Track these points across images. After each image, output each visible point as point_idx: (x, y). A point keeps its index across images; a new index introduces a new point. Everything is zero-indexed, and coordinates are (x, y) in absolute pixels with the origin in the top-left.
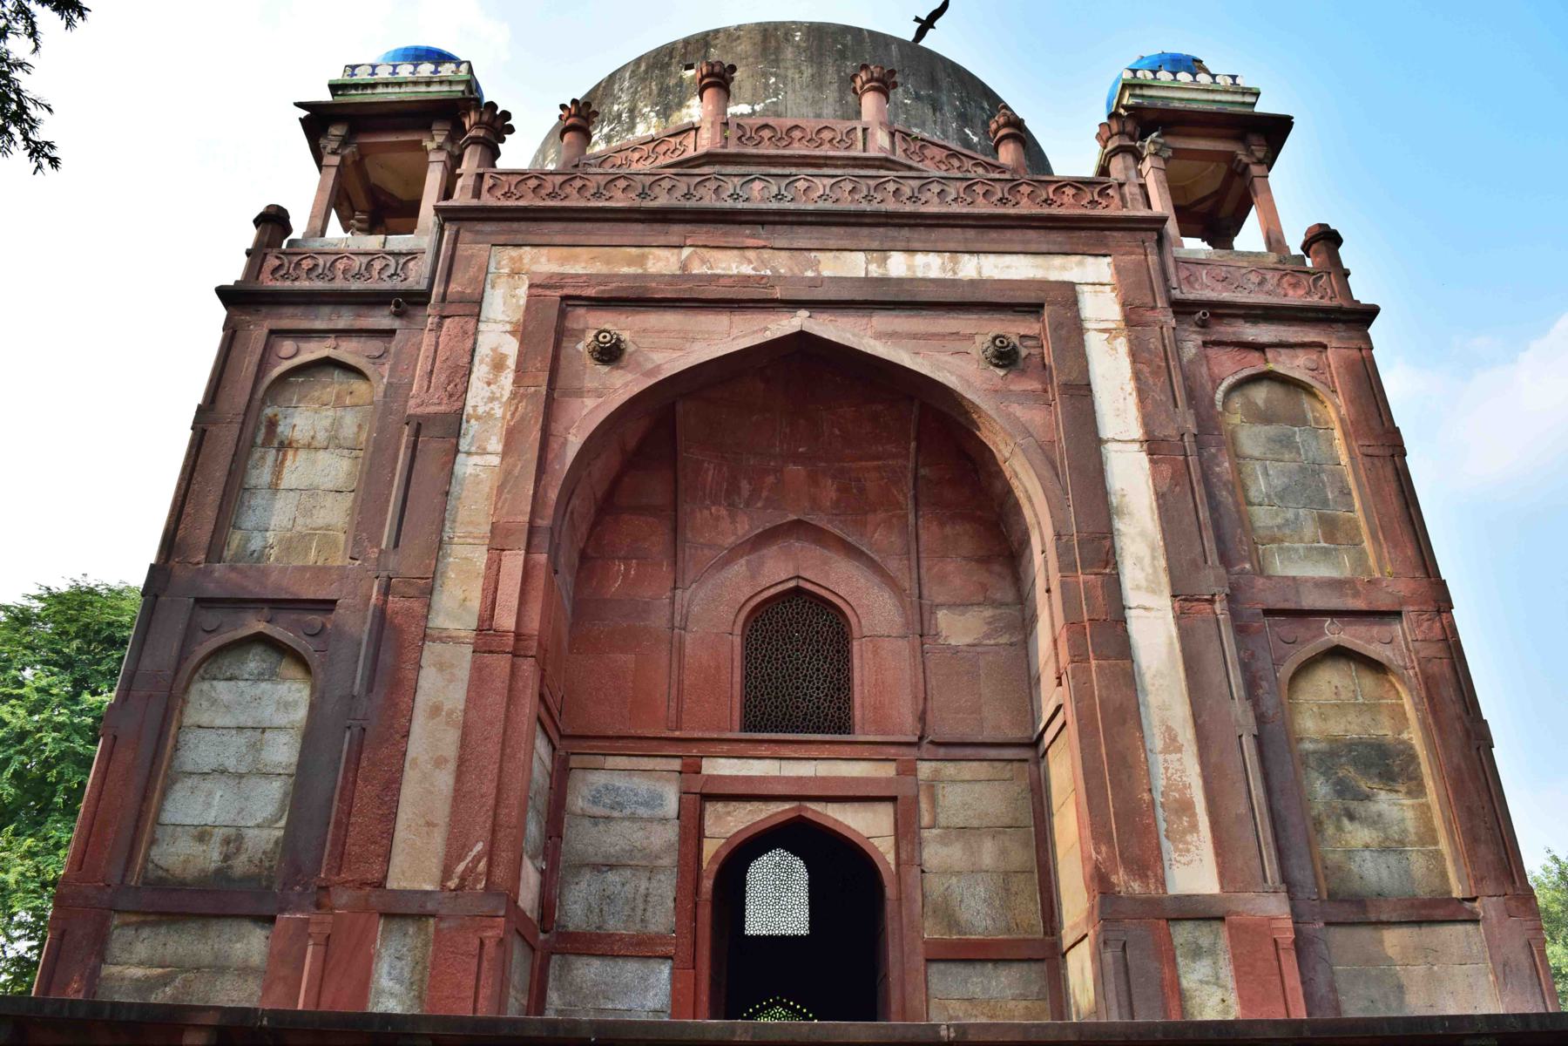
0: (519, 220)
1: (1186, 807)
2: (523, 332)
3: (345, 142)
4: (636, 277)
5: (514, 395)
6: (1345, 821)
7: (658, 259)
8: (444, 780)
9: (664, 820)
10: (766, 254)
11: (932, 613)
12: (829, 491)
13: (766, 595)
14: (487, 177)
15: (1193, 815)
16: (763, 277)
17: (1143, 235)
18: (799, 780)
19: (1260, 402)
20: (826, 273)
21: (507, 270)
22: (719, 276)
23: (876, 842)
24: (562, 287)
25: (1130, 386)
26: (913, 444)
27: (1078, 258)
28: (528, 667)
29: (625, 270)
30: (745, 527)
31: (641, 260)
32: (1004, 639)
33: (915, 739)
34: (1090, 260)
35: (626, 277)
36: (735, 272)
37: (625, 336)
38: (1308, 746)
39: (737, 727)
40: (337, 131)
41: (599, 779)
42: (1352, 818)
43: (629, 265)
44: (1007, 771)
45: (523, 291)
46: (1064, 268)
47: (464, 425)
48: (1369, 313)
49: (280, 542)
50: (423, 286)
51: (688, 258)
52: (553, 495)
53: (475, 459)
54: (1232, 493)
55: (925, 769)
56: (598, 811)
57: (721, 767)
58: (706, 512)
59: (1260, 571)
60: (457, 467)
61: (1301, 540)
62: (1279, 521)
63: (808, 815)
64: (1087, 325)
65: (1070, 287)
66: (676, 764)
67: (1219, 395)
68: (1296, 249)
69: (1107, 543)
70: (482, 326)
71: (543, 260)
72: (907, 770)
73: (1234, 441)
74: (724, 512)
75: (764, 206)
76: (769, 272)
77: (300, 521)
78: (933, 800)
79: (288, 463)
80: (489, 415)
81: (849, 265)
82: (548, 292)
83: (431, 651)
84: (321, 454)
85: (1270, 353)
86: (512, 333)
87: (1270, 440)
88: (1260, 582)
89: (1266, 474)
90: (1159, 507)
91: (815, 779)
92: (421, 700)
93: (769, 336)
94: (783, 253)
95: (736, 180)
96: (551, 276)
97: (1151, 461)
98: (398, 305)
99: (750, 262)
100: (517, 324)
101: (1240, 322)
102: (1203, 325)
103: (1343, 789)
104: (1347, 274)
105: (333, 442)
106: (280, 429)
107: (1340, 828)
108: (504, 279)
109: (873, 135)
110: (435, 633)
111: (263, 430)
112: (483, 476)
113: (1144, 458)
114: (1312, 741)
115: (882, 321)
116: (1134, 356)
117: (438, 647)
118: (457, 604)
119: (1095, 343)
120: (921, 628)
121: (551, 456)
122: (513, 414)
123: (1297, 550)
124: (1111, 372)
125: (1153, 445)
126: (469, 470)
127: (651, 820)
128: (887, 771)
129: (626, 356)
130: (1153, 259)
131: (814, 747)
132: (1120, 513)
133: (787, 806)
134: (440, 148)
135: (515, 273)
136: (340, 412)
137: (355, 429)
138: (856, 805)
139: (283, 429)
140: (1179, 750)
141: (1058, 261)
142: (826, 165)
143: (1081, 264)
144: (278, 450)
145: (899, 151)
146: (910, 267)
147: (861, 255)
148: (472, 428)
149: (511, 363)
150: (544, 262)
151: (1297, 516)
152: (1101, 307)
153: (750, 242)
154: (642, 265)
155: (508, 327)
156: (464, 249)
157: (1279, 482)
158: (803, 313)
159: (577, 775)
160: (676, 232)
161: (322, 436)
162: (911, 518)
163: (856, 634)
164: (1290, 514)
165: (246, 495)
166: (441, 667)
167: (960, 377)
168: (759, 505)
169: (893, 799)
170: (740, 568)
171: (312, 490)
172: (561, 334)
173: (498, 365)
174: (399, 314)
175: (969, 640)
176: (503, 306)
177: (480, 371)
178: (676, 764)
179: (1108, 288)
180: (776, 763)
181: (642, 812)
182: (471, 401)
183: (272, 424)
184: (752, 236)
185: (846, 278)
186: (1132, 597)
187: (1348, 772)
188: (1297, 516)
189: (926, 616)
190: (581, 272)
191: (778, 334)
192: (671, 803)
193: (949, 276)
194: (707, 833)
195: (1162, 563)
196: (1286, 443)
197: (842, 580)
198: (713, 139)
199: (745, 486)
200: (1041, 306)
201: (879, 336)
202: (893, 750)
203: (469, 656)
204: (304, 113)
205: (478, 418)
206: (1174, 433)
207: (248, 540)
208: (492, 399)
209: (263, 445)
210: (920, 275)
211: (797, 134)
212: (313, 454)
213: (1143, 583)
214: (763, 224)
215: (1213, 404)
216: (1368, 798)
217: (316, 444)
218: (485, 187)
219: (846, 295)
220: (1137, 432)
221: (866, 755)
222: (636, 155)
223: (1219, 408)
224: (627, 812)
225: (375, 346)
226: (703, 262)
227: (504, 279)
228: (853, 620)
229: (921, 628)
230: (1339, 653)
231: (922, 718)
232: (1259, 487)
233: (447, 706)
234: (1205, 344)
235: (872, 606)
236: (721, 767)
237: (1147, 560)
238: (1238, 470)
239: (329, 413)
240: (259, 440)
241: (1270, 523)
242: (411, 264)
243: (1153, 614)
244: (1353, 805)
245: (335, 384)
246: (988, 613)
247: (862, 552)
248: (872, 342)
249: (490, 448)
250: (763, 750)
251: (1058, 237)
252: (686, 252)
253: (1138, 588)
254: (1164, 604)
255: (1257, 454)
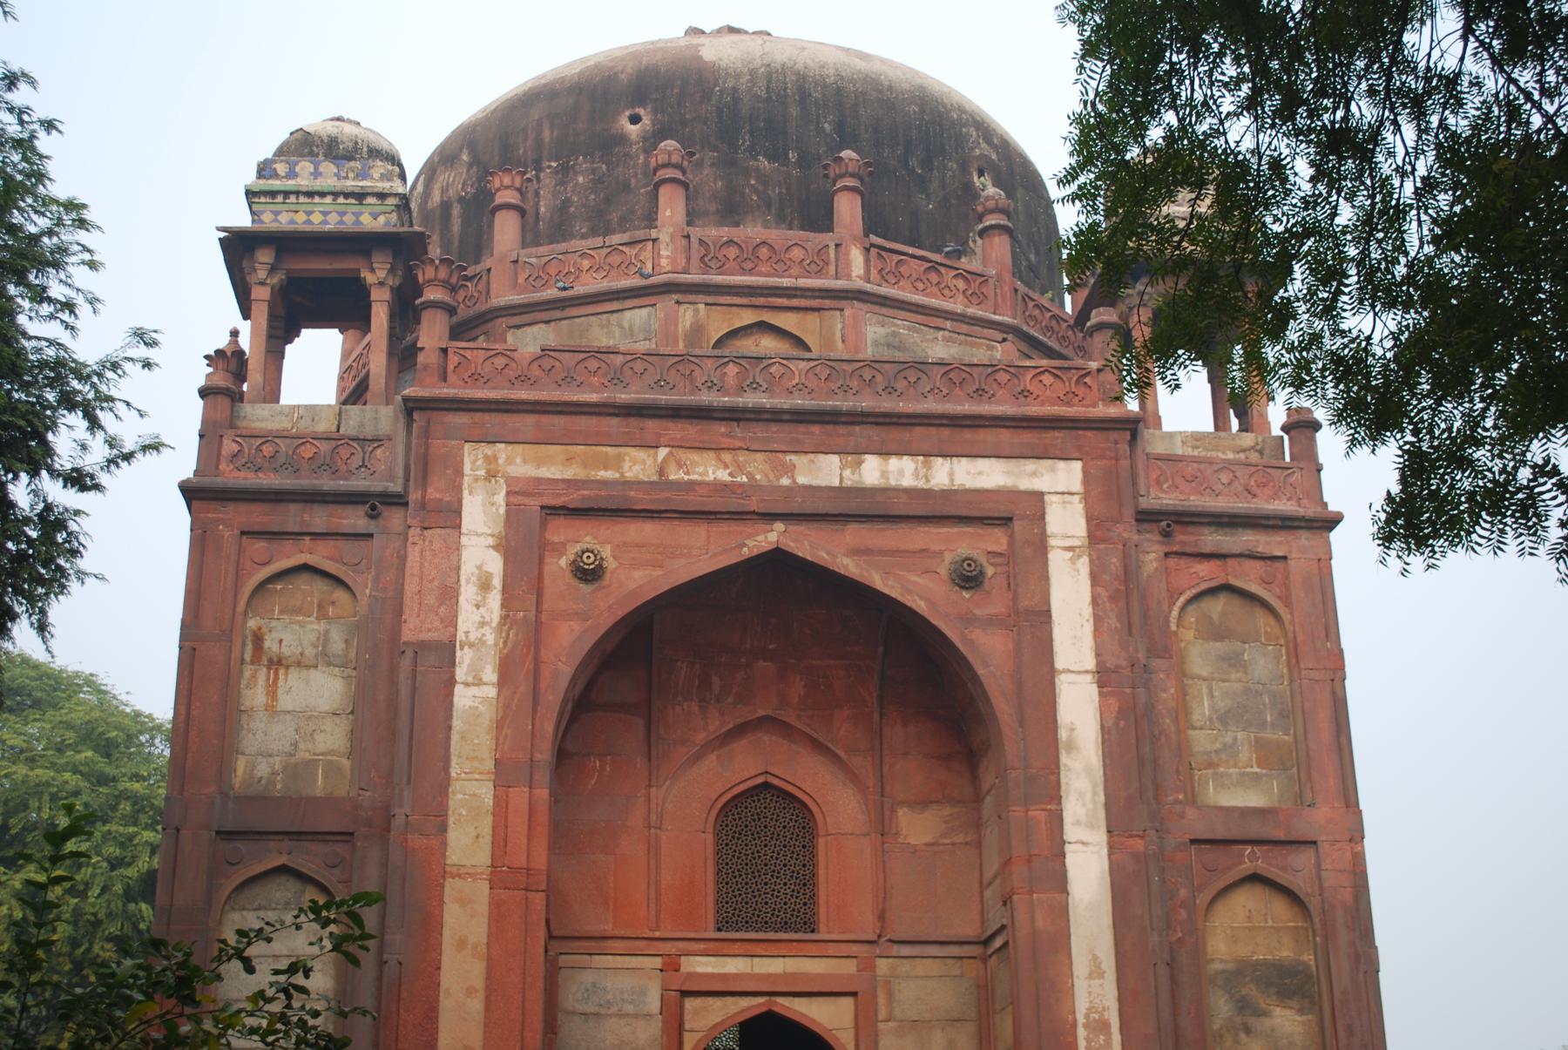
0: (490, 411)
1: (1104, 1026)
2: (505, 546)
3: (273, 269)
4: (614, 483)
5: (504, 619)
6: (1242, 1035)
7: (634, 461)
8: (476, 1005)
9: (649, 1015)
10: (742, 457)
11: (893, 811)
12: (797, 688)
13: (735, 791)
14: (450, 352)
15: (1109, 1034)
16: (741, 485)
17: (1113, 435)
18: (769, 976)
19: (1215, 616)
20: (802, 480)
21: (482, 473)
22: (692, 483)
23: (838, 1034)
24: (541, 495)
25: (1088, 611)
26: (881, 650)
27: (1049, 462)
28: (539, 900)
29: (604, 474)
30: (716, 724)
31: (617, 463)
32: (959, 839)
33: (874, 938)
34: (1061, 464)
35: (604, 483)
36: (711, 477)
37: (606, 552)
38: (1217, 966)
39: (712, 926)
40: (265, 256)
41: (588, 978)
42: (1248, 1031)
43: (606, 468)
44: (955, 968)
45: (500, 498)
46: (1034, 474)
47: (458, 653)
48: (1333, 521)
49: (285, 768)
50: (396, 487)
51: (665, 460)
52: (549, 728)
53: (473, 690)
54: (1176, 721)
55: (883, 966)
56: (590, 1008)
57: (703, 965)
58: (678, 709)
59: (1192, 800)
60: (456, 699)
61: (1236, 766)
62: (1218, 745)
63: (777, 1009)
64: (1052, 542)
65: (1039, 496)
66: (657, 962)
67: (1175, 613)
68: (1276, 431)
69: (1053, 778)
70: (464, 540)
71: (518, 460)
72: (868, 966)
73: (1182, 660)
74: (696, 708)
75: (740, 401)
76: (745, 479)
77: (302, 746)
78: (890, 997)
79: (281, 682)
80: (482, 642)
81: (824, 471)
82: (527, 501)
83: (451, 888)
84: (312, 671)
85: (1230, 562)
86: (496, 548)
87: (1221, 658)
88: (1191, 813)
89: (1211, 696)
90: (1103, 743)
91: (785, 977)
92: (446, 933)
93: (746, 553)
94: (759, 456)
95: (709, 362)
96: (530, 480)
97: (1101, 694)
98: (373, 508)
99: (726, 467)
100: (499, 537)
101: (1206, 530)
102: (1166, 534)
103: (1244, 1006)
104: (1319, 471)
105: (325, 658)
106: (267, 644)
107: (1237, 1042)
108: (481, 483)
109: (848, 254)
110: (454, 870)
111: (249, 647)
112: (481, 708)
113: (1094, 689)
114: (1222, 961)
115: (854, 534)
116: (1095, 579)
117: (458, 883)
118: (468, 841)
119: (1057, 561)
120: (883, 829)
121: (543, 685)
122: (505, 643)
123: (1229, 775)
124: (1071, 595)
125: (1104, 676)
126: (468, 703)
127: (636, 1016)
128: (849, 967)
129: (608, 575)
130: (1124, 463)
131: (783, 945)
132: (1072, 746)
133: (761, 1000)
134: (381, 284)
135: (491, 475)
136: (323, 626)
137: (342, 645)
138: (821, 999)
139: (270, 644)
140: (1101, 975)
141: (1030, 465)
142: (795, 296)
143: (1052, 470)
144: (269, 669)
145: (874, 272)
146: (884, 474)
147: (835, 459)
148: (464, 658)
149: (497, 582)
150: (520, 463)
151: (1235, 739)
152: (1066, 522)
153: (726, 442)
154: (619, 468)
155: (491, 541)
156: (435, 442)
157: (1222, 705)
158: (779, 526)
159: (564, 974)
160: (651, 425)
161: (310, 652)
162: (876, 717)
163: (822, 831)
164: (1228, 739)
165: (244, 718)
166: (463, 902)
167: (928, 600)
168: (730, 700)
169: (854, 994)
170: (710, 762)
171: (308, 716)
172: (543, 549)
173: (485, 586)
174: (372, 517)
175: (927, 839)
176: (481, 514)
177: (468, 593)
178: (658, 962)
179: (1076, 498)
180: (748, 960)
181: (629, 1008)
182: (463, 625)
183: (258, 639)
184: (728, 435)
185: (819, 488)
186: (1071, 832)
187: (1250, 990)
188: (1235, 739)
189: (887, 813)
190: (559, 476)
191: (756, 552)
192: (653, 1002)
193: (921, 484)
194: (687, 1027)
195: (1101, 798)
196: (1234, 661)
197: (809, 776)
198: (673, 259)
199: (716, 681)
200: (1011, 519)
201: (855, 552)
202: (855, 948)
203: (486, 891)
204: (223, 234)
205: (471, 645)
206: (1124, 663)
207: (254, 767)
208: (482, 624)
209: (252, 663)
210: (893, 482)
211: (764, 251)
212: (304, 672)
213: (1083, 819)
214: (738, 420)
215: (1167, 621)
216: (1266, 1014)
217: (305, 661)
218: (451, 367)
219: (821, 507)
220: (1090, 663)
221: (830, 953)
222: (586, 263)
223: (1173, 628)
224: (614, 1010)
225: (350, 549)
226: (680, 465)
227: (481, 483)
228: (818, 817)
229: (883, 829)
230: (1255, 878)
231: (881, 917)
232: (1202, 709)
233: (472, 940)
234: (1167, 555)
235: (838, 804)
236: (703, 965)
237: (1089, 796)
238: (1183, 693)
239: (314, 627)
240: (248, 657)
241: (1209, 747)
242: (379, 452)
243: (1091, 848)
244: (1252, 1021)
245: (312, 589)
246: (946, 811)
247: (828, 749)
248: (846, 561)
249: (486, 679)
250: (736, 947)
251: (1028, 437)
252: (663, 452)
253: (1077, 823)
254: (1099, 837)
255: (1204, 673)
